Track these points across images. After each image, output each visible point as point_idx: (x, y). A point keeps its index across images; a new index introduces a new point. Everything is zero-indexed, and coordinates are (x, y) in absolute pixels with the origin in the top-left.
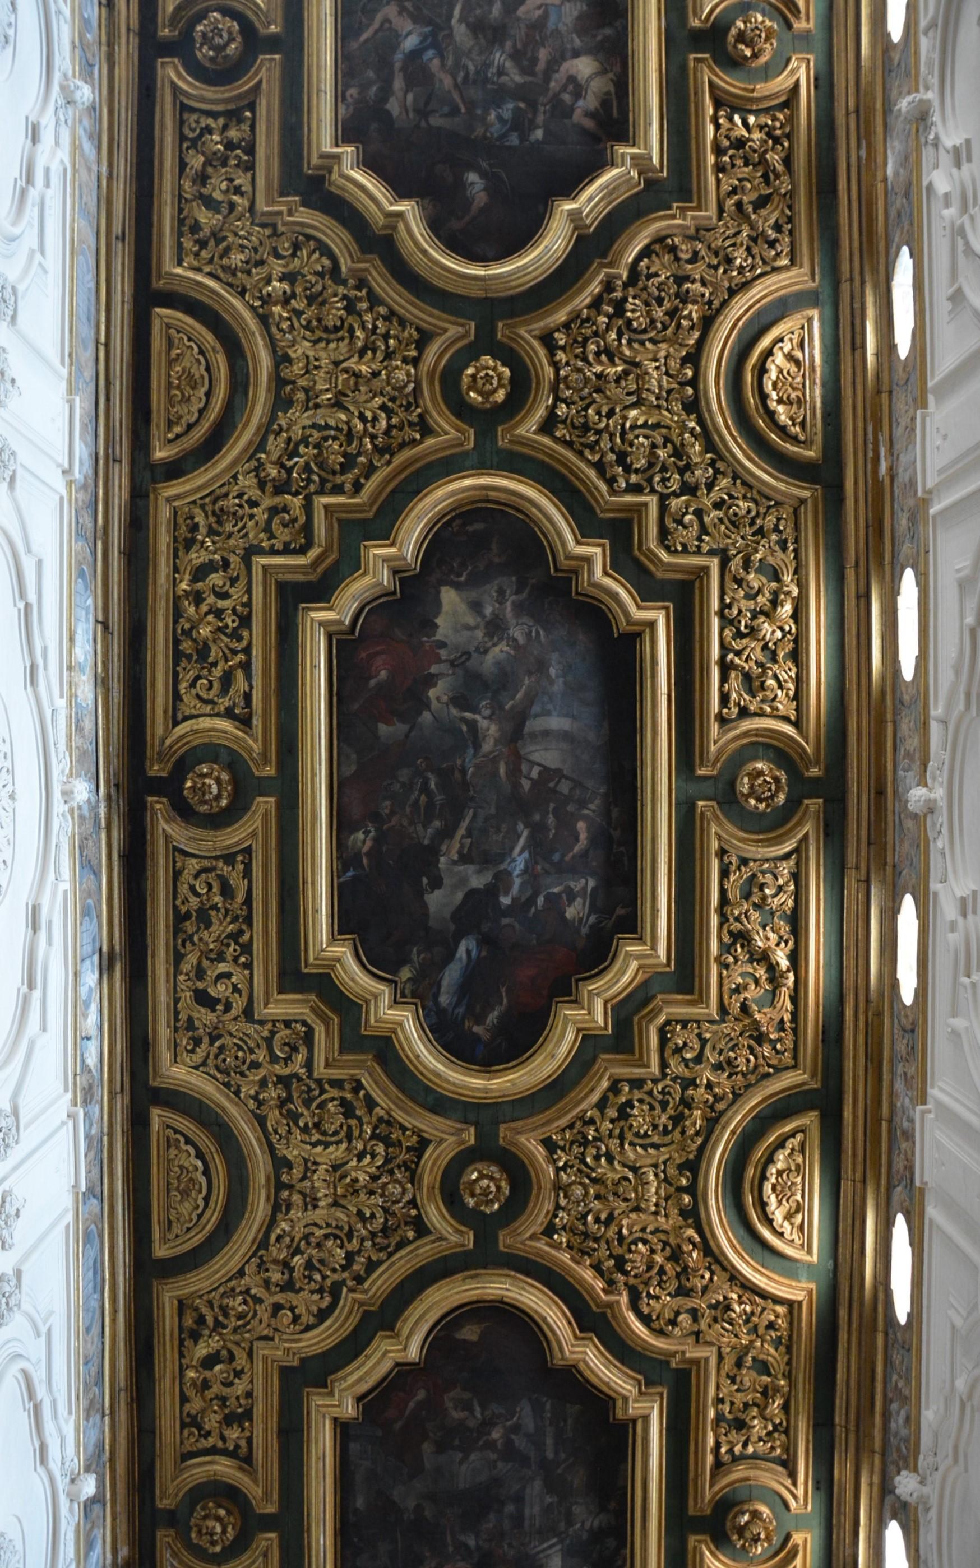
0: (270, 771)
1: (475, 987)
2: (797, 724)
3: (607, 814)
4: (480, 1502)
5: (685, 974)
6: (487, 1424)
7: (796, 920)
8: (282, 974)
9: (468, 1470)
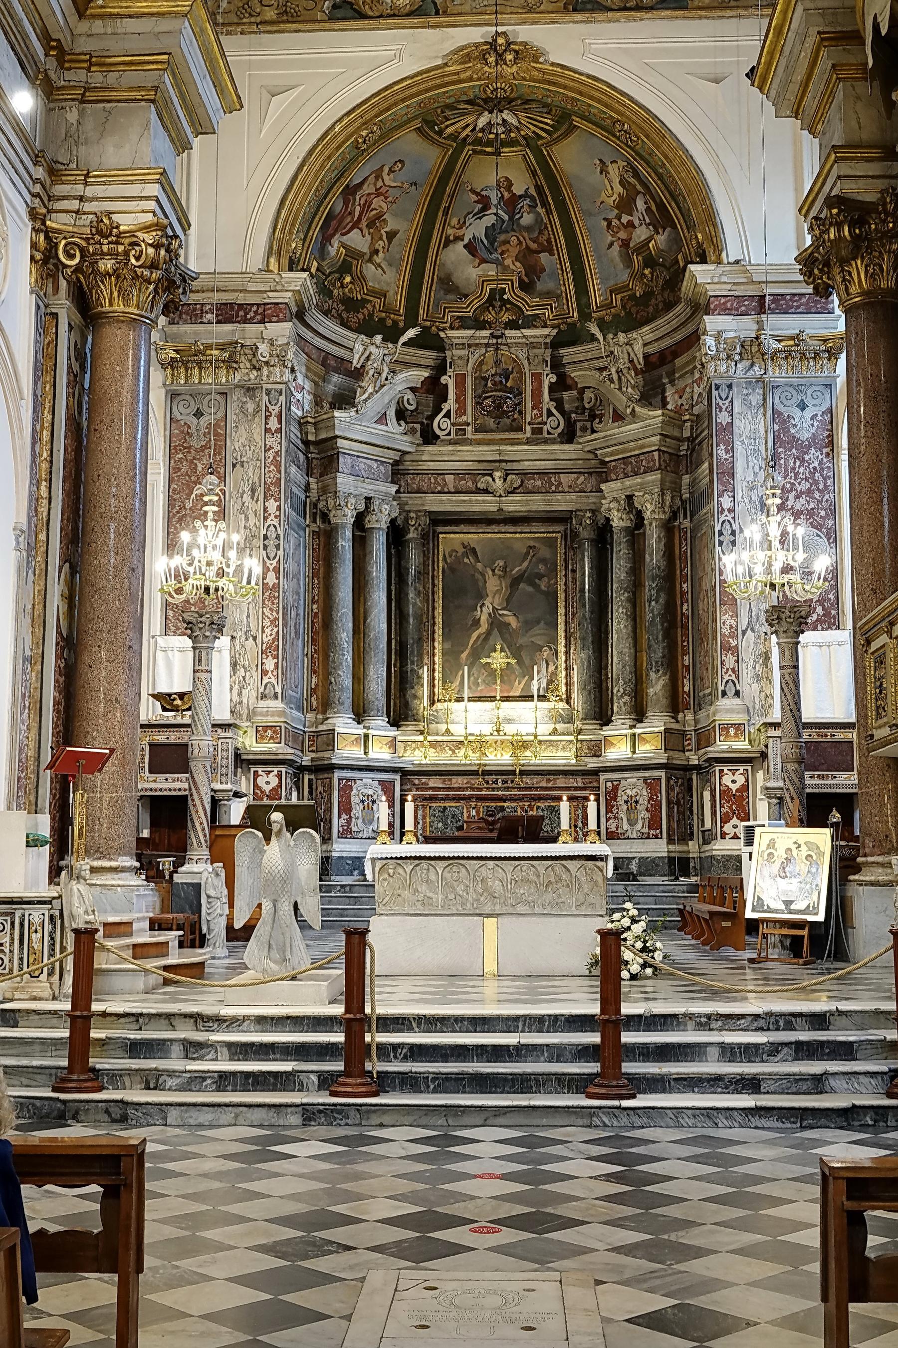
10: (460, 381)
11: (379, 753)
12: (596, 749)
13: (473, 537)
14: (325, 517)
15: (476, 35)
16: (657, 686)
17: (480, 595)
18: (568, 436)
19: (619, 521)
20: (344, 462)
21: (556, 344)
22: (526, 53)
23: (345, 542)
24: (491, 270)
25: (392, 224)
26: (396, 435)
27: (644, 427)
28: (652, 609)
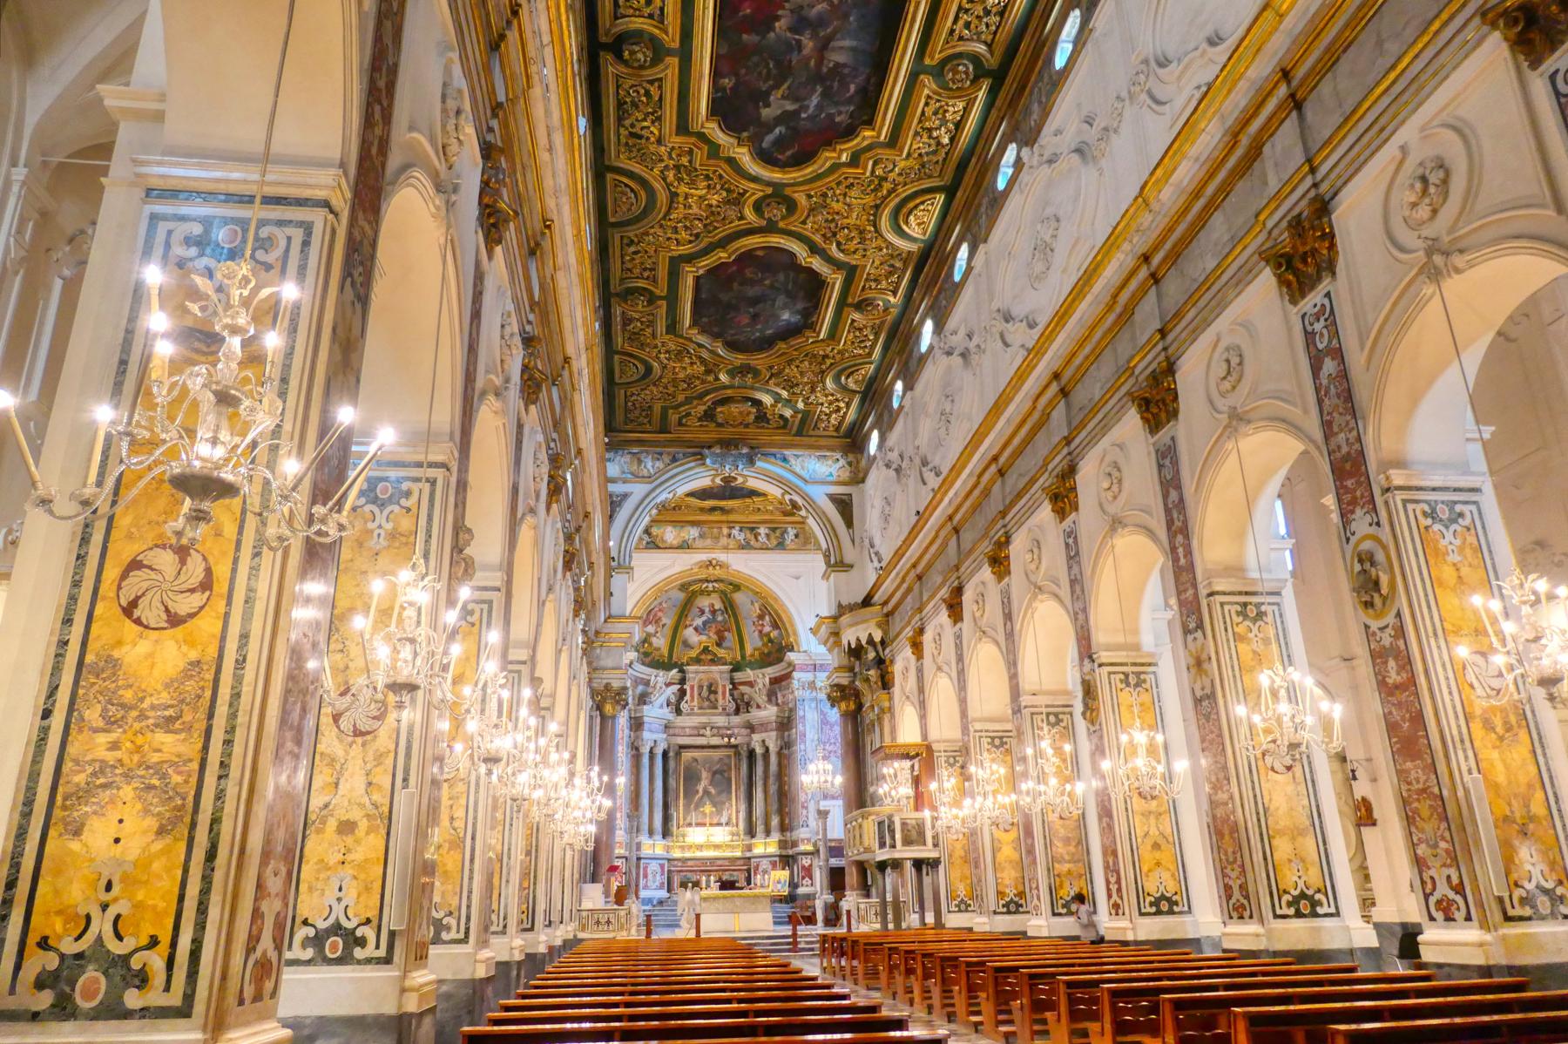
0: (676, 45)
1: (780, 143)
2: (989, 46)
3: (868, 79)
4: (755, 301)
5: (894, 141)
6: (763, 279)
7: (959, 125)
8: (678, 127)
9: (752, 292)
10: (692, 688)
11: (659, 851)
12: (749, 848)
13: (696, 754)
14: (637, 749)
15: (704, 557)
16: (775, 821)
17: (699, 779)
18: (737, 712)
19: (759, 750)
20: (646, 726)
21: (732, 671)
22: (721, 565)
23: (645, 760)
24: (704, 638)
25: (664, 620)
26: (667, 713)
27: (769, 713)
28: (773, 788)
